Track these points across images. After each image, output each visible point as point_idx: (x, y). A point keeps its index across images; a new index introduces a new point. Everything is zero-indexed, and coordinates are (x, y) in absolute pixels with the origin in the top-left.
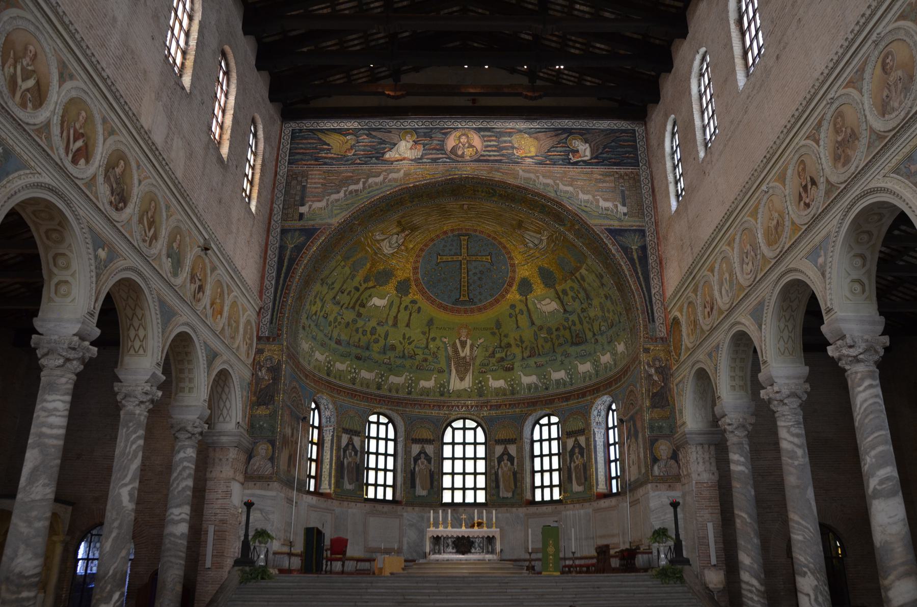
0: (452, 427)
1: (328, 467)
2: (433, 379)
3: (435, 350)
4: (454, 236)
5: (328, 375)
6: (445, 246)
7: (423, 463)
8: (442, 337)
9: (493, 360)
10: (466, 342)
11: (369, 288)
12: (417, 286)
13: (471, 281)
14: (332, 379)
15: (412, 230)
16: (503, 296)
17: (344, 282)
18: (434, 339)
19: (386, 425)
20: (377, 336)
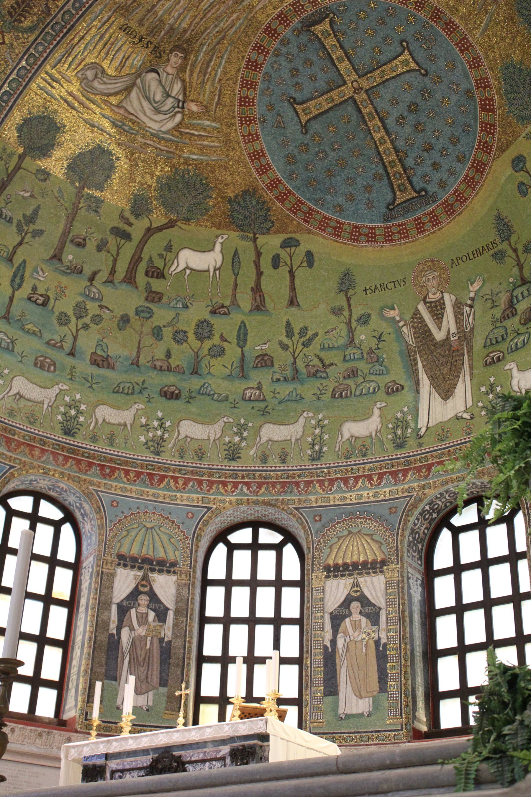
0: (451, 527)
1: (79, 654)
2: (377, 412)
3: (373, 343)
4: (298, 32)
5: (68, 432)
6: (294, 72)
7: (356, 626)
8: (382, 308)
9: (514, 322)
10: (441, 303)
11: (160, 229)
12: (282, 201)
13: (400, 143)
14: (78, 441)
15: (186, 52)
16: (486, 147)
17: (72, 217)
18: (364, 319)
19: (278, 548)
20: (216, 340)
